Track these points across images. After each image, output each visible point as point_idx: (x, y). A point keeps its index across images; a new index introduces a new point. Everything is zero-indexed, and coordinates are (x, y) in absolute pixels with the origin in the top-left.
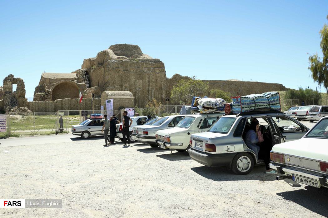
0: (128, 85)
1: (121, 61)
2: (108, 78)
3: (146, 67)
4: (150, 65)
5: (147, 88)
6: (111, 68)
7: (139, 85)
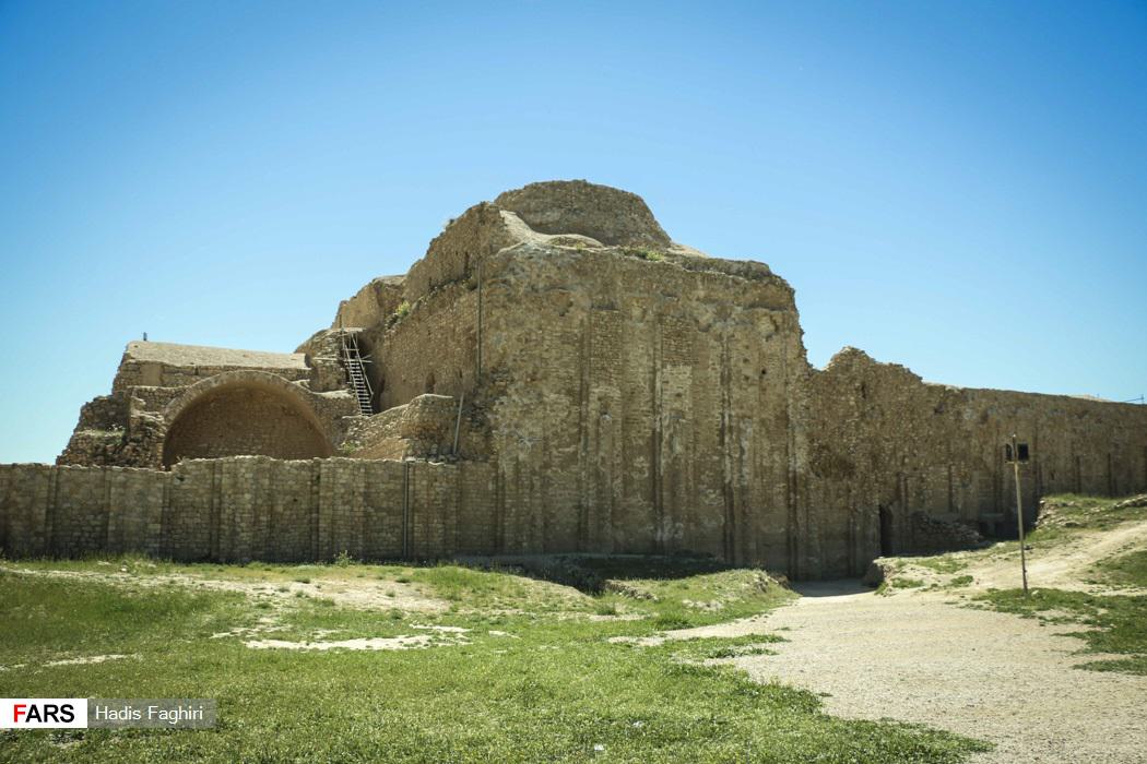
0: (616, 394)
1: (579, 256)
2: (501, 342)
3: (707, 300)
4: (727, 287)
5: (716, 413)
6: (522, 290)
7: (679, 395)
